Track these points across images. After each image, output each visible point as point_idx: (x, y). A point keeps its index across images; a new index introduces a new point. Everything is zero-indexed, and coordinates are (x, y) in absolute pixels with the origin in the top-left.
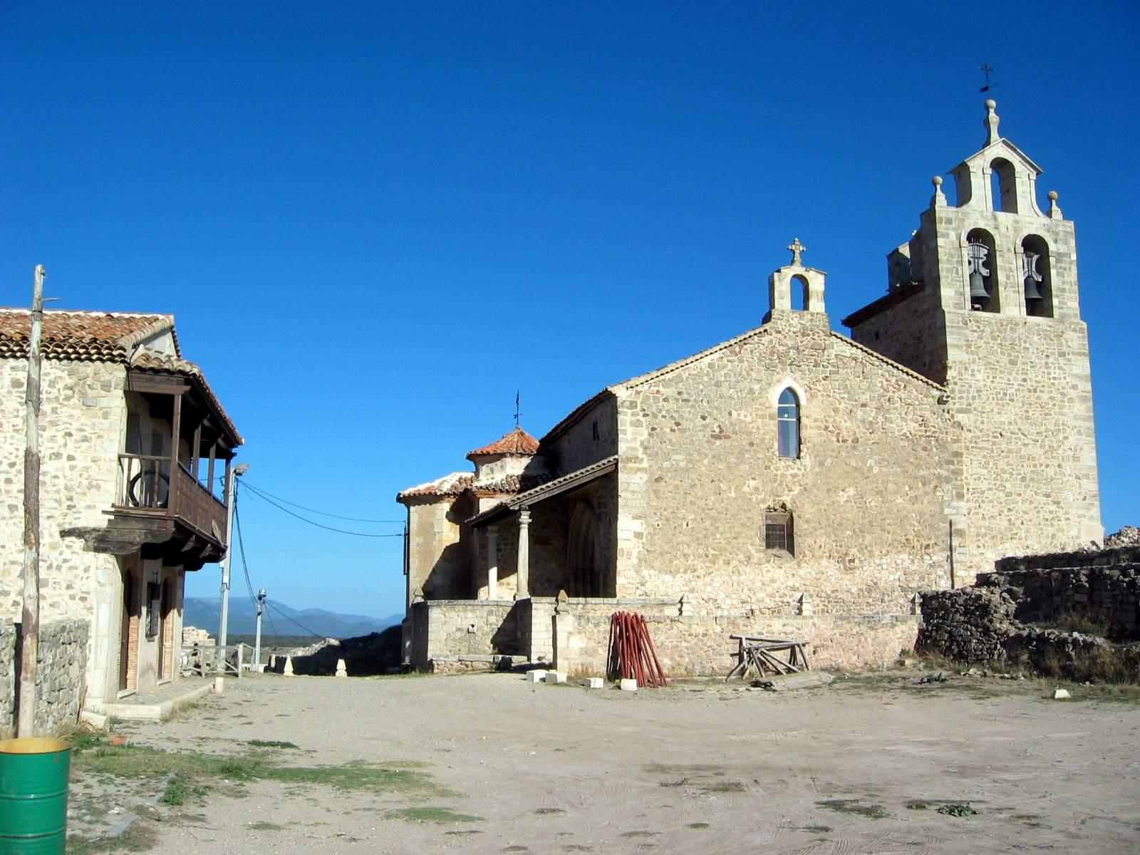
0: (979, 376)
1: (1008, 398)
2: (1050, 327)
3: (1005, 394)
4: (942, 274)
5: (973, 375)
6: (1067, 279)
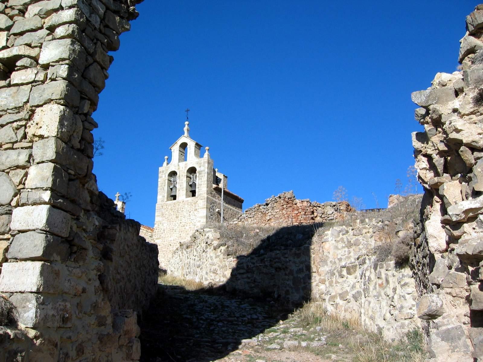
0: (165, 225)
1: (174, 231)
2: (193, 200)
3: (173, 230)
4: (159, 191)
5: (163, 225)
6: (203, 180)
